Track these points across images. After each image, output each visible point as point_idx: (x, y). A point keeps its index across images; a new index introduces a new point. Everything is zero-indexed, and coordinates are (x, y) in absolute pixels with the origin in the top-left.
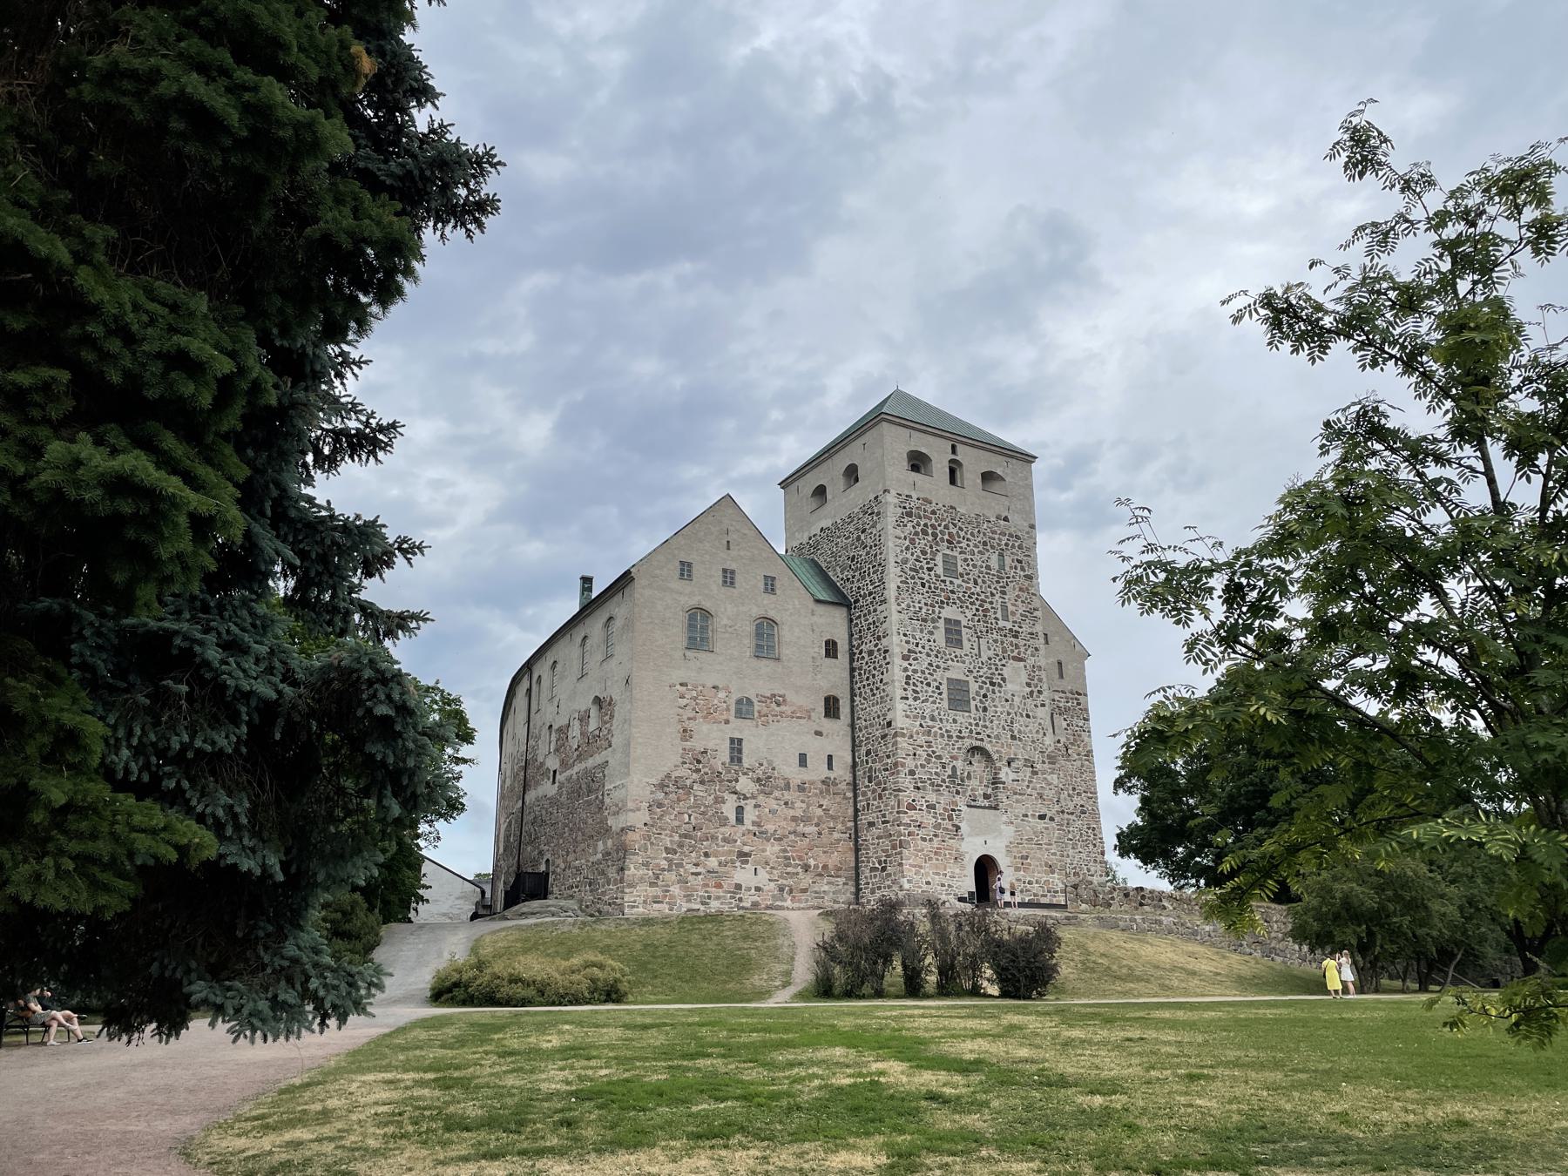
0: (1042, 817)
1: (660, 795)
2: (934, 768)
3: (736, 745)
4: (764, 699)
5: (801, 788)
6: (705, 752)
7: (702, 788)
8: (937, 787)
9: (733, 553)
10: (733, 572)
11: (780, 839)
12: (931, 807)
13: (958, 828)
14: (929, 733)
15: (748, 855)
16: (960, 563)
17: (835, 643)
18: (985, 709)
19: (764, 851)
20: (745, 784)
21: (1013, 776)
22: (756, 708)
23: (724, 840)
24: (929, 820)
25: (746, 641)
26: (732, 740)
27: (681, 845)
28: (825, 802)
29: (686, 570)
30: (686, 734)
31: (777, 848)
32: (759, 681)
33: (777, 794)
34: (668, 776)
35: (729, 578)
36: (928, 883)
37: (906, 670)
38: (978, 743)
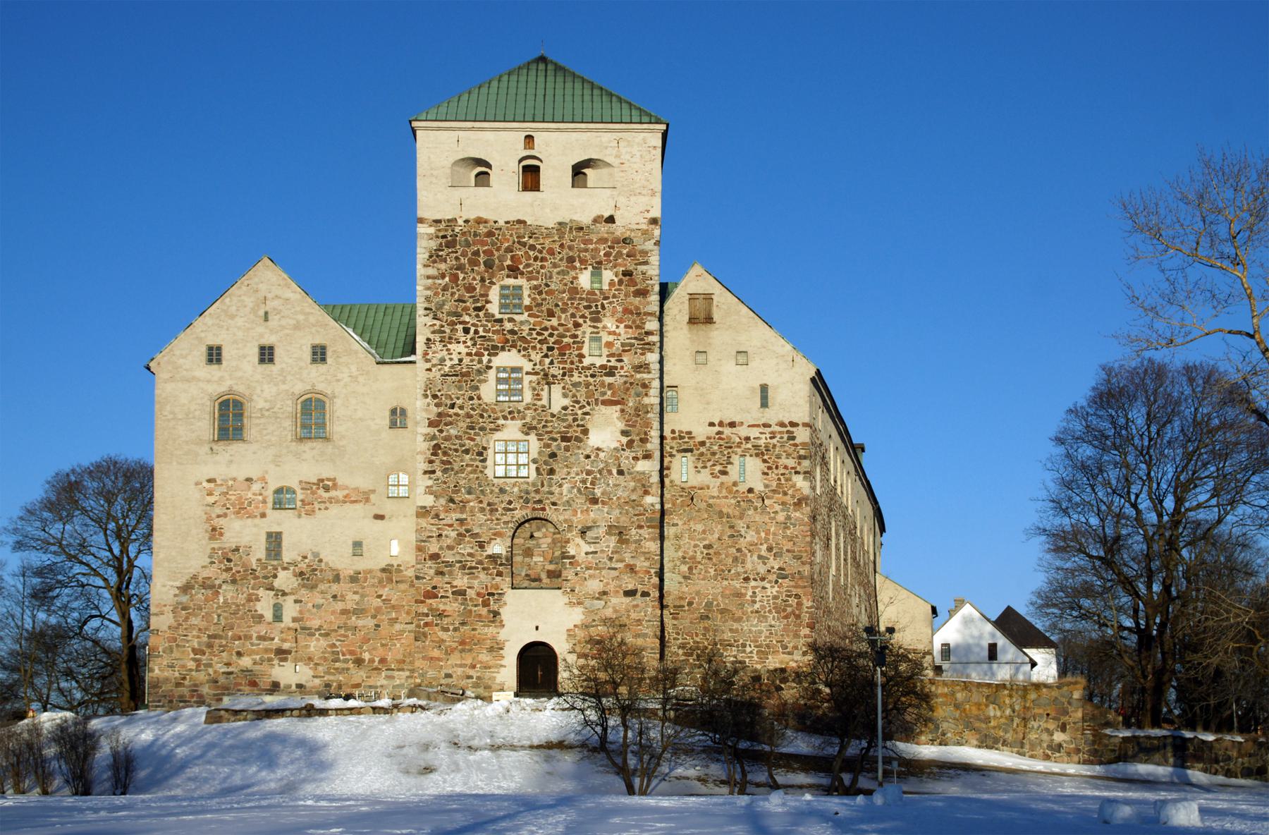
0: (630, 593)
1: (184, 599)
2: (465, 548)
3: (275, 540)
4: (306, 486)
5: (354, 579)
6: (237, 549)
7: (230, 587)
8: (469, 570)
9: (274, 321)
10: (271, 348)
11: (327, 635)
12: (462, 593)
13: (496, 614)
14: (463, 510)
15: (288, 652)
16: (526, 292)
17: (403, 412)
18: (552, 472)
19: (307, 646)
20: (285, 580)
21: (586, 548)
22: (300, 495)
23: (260, 638)
24: (452, 607)
25: (288, 423)
26: (269, 535)
27: (210, 646)
28: (385, 592)
29: (214, 355)
30: (215, 532)
31: (323, 643)
32: (303, 466)
33: (322, 587)
34: (195, 577)
35: (267, 354)
36: (448, 676)
37: (433, 438)
38: (541, 514)
